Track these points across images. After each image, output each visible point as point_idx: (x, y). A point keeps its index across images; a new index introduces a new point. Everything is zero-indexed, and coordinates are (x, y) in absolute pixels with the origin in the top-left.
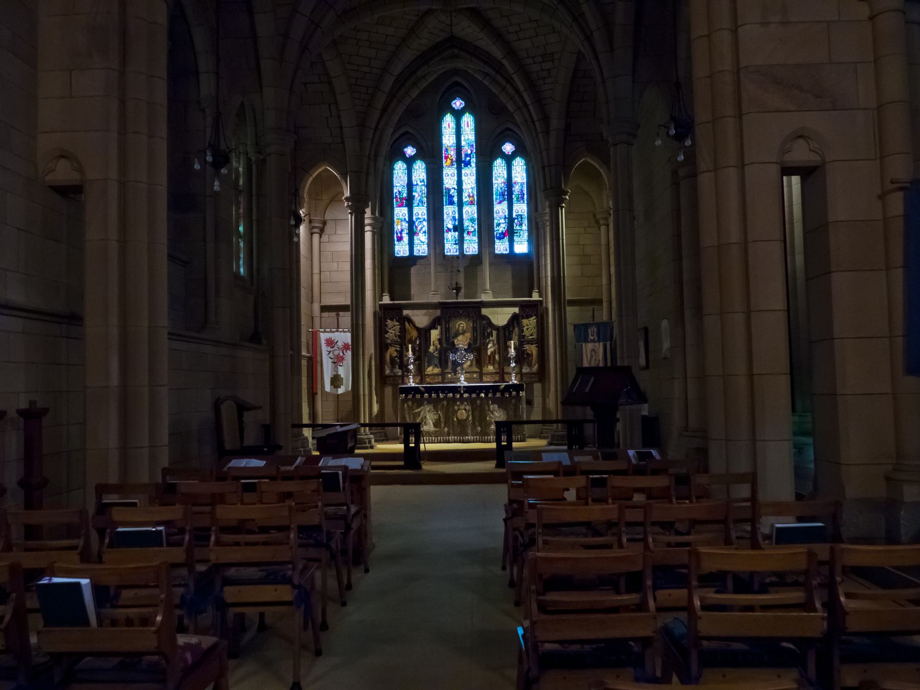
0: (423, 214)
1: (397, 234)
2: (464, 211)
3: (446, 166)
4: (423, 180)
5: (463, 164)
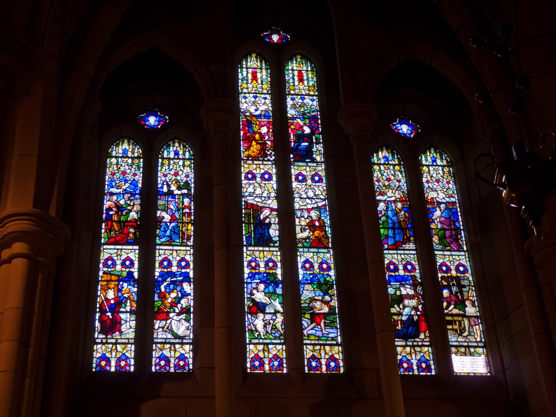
0: (183, 264)
1: (103, 312)
2: (300, 260)
3: (249, 156)
4: (187, 184)
5: (292, 156)
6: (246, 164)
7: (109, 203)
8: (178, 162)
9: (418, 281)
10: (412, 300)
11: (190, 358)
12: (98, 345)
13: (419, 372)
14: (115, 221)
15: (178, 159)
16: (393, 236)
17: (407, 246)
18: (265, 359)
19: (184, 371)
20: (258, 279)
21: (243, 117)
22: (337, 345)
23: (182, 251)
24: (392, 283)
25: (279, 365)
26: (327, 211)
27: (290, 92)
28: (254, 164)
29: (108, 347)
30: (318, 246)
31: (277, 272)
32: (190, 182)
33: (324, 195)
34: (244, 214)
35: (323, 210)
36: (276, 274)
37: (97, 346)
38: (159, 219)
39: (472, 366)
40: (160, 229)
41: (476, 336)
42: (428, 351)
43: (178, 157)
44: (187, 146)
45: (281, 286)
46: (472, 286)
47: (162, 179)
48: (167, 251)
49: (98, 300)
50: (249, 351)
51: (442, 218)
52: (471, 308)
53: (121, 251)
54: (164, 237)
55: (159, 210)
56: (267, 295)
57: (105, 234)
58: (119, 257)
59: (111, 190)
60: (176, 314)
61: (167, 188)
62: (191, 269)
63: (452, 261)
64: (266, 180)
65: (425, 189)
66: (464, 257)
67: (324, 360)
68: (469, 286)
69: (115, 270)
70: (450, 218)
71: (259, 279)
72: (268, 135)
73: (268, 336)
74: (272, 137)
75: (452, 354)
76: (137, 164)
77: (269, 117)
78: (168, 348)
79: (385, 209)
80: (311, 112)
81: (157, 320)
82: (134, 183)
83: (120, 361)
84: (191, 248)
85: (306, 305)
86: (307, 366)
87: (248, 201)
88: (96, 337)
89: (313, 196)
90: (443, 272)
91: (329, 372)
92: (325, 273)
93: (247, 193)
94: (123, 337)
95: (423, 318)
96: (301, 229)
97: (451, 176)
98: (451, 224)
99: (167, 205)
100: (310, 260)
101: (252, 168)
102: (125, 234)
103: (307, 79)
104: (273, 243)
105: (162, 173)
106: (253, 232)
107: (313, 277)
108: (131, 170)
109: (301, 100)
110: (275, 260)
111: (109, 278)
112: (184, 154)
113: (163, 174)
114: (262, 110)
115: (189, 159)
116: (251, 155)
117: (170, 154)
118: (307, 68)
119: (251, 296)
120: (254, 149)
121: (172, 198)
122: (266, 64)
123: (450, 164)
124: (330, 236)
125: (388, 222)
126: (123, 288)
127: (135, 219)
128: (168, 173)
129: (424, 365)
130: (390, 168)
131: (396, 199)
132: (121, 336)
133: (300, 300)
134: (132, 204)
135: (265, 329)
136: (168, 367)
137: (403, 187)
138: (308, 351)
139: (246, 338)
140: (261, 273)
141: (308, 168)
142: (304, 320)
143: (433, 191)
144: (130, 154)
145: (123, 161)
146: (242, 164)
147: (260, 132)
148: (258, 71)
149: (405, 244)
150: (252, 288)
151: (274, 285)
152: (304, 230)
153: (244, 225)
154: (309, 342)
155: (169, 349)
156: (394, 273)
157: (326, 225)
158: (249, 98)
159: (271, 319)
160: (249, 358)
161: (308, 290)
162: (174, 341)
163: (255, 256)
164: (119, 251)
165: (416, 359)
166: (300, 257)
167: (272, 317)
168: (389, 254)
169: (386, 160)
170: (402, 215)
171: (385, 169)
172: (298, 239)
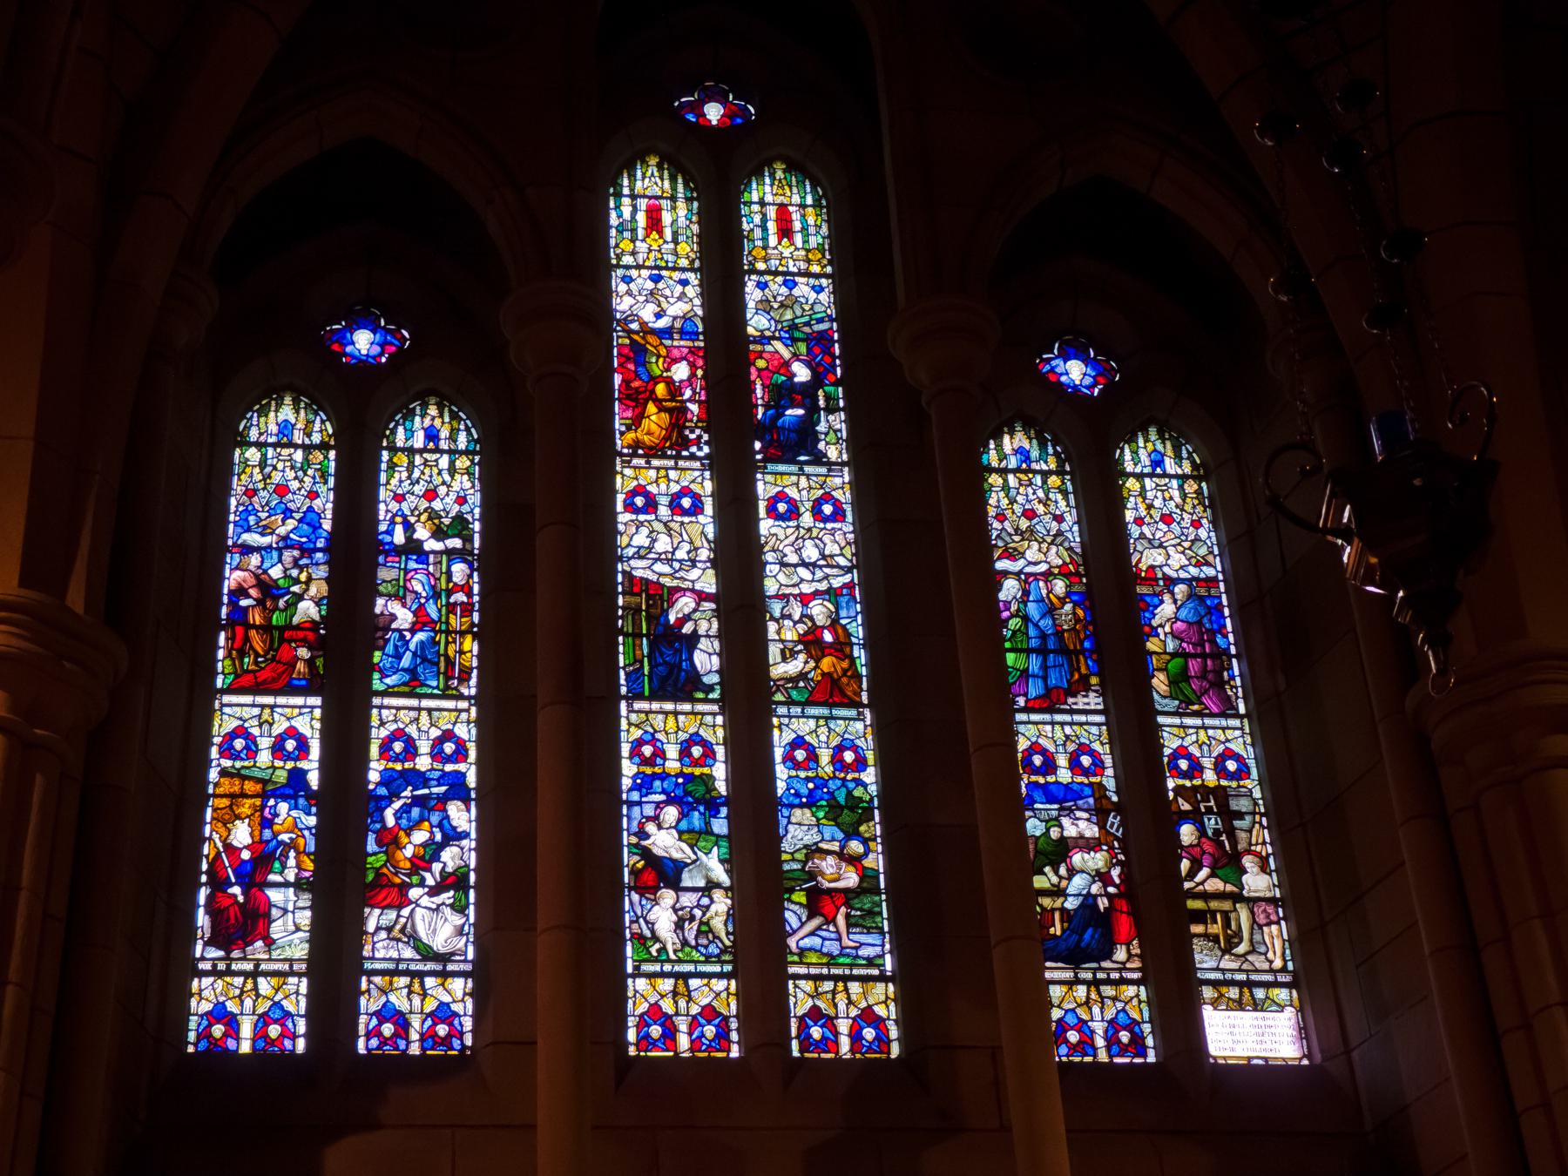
0: (449, 748)
1: (218, 883)
2: (780, 740)
3: (636, 445)
4: (461, 523)
5: (758, 445)
6: (631, 467)
7: (238, 574)
8: (436, 461)
9: (1109, 799)
10: (1092, 853)
11: (465, 1015)
12: (204, 980)
13: (1111, 1057)
14: (254, 626)
15: (437, 450)
16: (1041, 674)
17: (1080, 702)
18: (680, 1018)
19: (449, 1053)
20: (660, 793)
21: (620, 334)
22: (882, 978)
23: (445, 713)
24: (1037, 806)
25: (717, 1036)
26: (856, 602)
27: (754, 265)
28: (650, 468)
29: (232, 985)
30: (831, 700)
31: (714, 774)
32: (469, 517)
33: (850, 557)
34: (622, 608)
35: (847, 598)
36: (711, 777)
37: (200, 981)
38: (381, 620)
39: (1259, 1039)
40: (382, 649)
41: (1270, 955)
42: (1137, 996)
43: (437, 445)
44: (461, 414)
45: (724, 811)
46: (1262, 815)
47: (389, 507)
48: (402, 712)
49: (206, 851)
50: (635, 996)
51: (1179, 623)
52: (1259, 877)
53: (272, 712)
54: (394, 673)
55: (382, 595)
56: (685, 837)
57: (228, 662)
58: (266, 727)
59: (245, 536)
60: (426, 890)
61: (405, 532)
62: (471, 764)
63: (1204, 743)
64: (685, 512)
65: (1132, 541)
66: (1238, 733)
67: (846, 1020)
68: (1254, 813)
69: (254, 766)
70: (1200, 623)
71: (664, 792)
72: (691, 385)
73: (689, 954)
74: (703, 392)
75: (1204, 1006)
76: (320, 464)
77: (693, 335)
78: (405, 987)
79: (1018, 596)
80: (813, 322)
81: (373, 907)
82: (310, 520)
83: (266, 1025)
84: (471, 705)
85: (796, 866)
86: (798, 1037)
87: (634, 573)
88: (198, 955)
89: (818, 560)
90: (1180, 774)
91: (858, 1056)
92: (849, 777)
93: (630, 548)
94: (275, 955)
95: (1123, 905)
96: (783, 652)
97: (1205, 507)
98: (1205, 641)
99: (405, 580)
100: (807, 738)
101: (645, 478)
102: (284, 664)
103: (803, 228)
104: (703, 692)
105: (391, 491)
106: (646, 659)
107: (816, 787)
108: (301, 481)
109: (786, 287)
110: (710, 739)
111: (236, 789)
112: (453, 438)
113: (395, 493)
114: (674, 314)
115: (466, 452)
116: (644, 443)
117: (413, 436)
118: (801, 198)
119: (640, 839)
120: (652, 425)
121: (417, 561)
122: (686, 185)
123: (1202, 472)
124: (864, 673)
125: (1027, 634)
126: (276, 815)
127: (313, 622)
128: (408, 492)
129: (1125, 1037)
130: (1033, 480)
131: (1049, 569)
132: (269, 951)
133: (780, 852)
134: (303, 577)
135: (681, 935)
136: (404, 1042)
137: (1069, 535)
138: (800, 995)
139: (625, 959)
140: (669, 775)
141: (803, 480)
142: (788, 909)
143: (1155, 547)
144: (298, 437)
145: (280, 455)
146: (618, 468)
147: (668, 377)
148: (665, 204)
149: (1075, 696)
150: (644, 817)
151: (705, 809)
152: (791, 656)
153: (621, 639)
154: (802, 970)
155: (405, 991)
156: (1044, 776)
157: (854, 640)
158: (639, 281)
159: (696, 907)
160: (634, 1015)
161: (800, 824)
162: (420, 967)
163: (652, 726)
164: (267, 711)
165: (1103, 1020)
166: (781, 730)
167: (699, 901)
168: (1029, 722)
169: (1023, 458)
170: (1067, 615)
171: (1021, 485)
172: (774, 681)
